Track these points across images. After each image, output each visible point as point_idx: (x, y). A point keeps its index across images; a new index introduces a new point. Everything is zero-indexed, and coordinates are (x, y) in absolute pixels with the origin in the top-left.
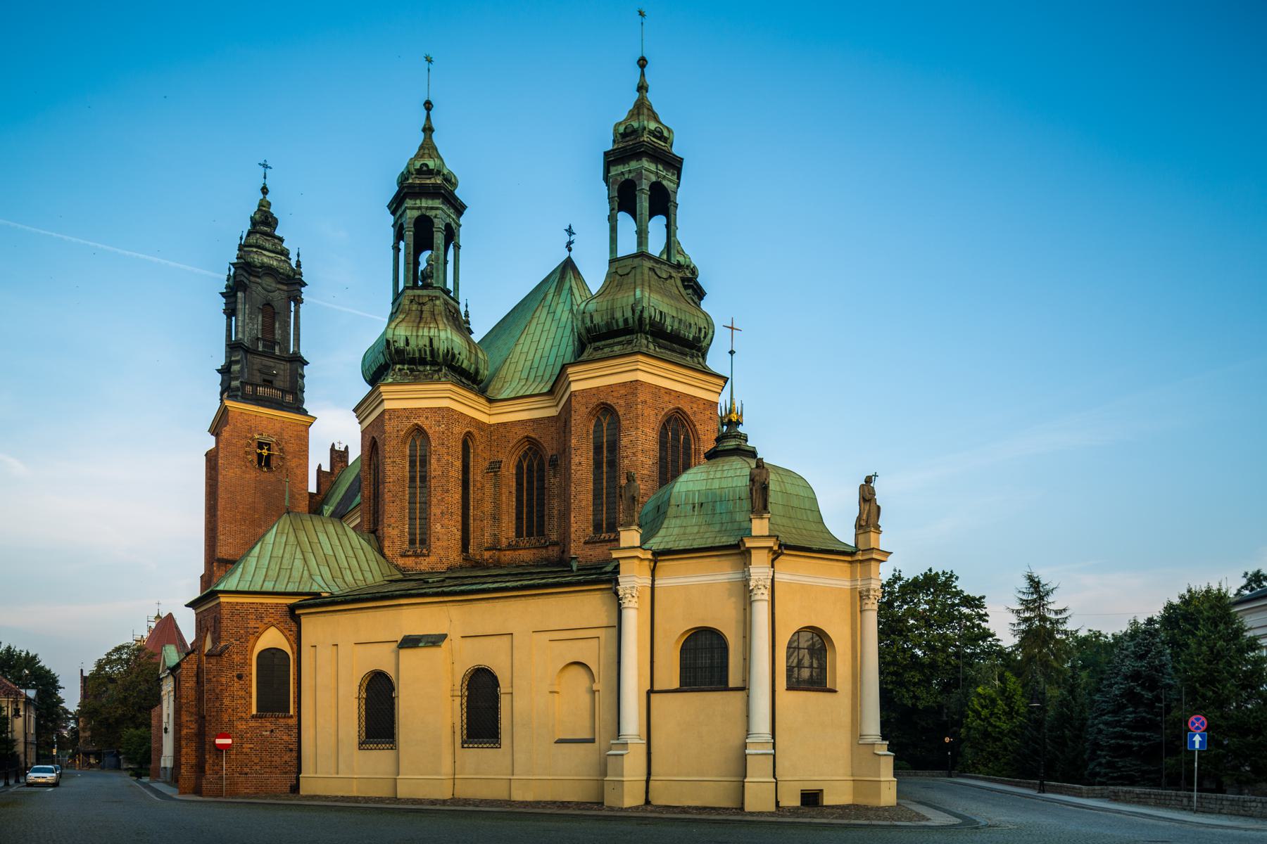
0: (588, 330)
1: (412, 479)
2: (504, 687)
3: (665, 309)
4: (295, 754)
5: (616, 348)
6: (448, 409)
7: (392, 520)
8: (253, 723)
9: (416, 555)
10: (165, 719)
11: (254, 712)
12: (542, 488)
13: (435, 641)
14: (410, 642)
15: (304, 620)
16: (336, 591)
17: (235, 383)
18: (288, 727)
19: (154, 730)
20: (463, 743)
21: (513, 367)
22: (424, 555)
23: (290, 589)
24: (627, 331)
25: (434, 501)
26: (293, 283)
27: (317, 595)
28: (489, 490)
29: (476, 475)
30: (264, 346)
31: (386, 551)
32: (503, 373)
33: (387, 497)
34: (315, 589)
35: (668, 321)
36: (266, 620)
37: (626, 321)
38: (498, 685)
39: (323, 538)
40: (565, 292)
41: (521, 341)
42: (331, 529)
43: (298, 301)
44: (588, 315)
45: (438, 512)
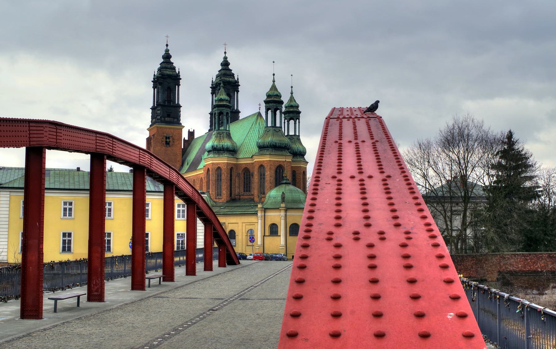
3: (277, 142)
17: (159, 117)
24: (267, 147)
26: (175, 79)
29: (233, 177)
43: (179, 85)
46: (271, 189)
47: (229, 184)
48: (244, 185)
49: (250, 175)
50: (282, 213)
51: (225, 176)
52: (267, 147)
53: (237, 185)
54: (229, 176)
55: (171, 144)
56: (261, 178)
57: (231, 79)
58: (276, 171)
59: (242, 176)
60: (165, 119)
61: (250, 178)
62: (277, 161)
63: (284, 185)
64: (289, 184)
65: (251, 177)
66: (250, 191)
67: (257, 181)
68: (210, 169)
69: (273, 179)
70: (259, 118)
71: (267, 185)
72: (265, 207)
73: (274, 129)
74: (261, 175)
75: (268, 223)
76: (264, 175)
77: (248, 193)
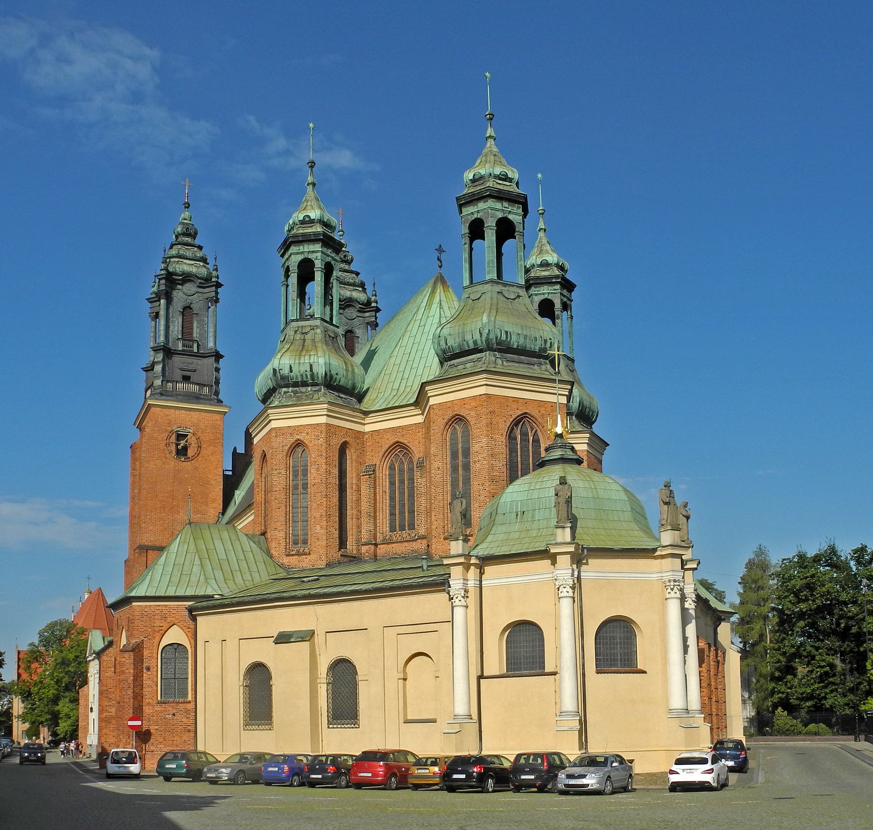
0: (444, 352)
1: (296, 487)
3: (510, 330)
4: (192, 734)
5: (468, 365)
6: (328, 425)
7: (279, 524)
8: (158, 708)
9: (298, 554)
10: (91, 700)
11: (159, 699)
12: (412, 489)
13: (308, 636)
14: (283, 638)
15: (199, 619)
16: (226, 592)
18: (187, 711)
19: (81, 710)
20: (329, 723)
21: (387, 377)
22: (306, 554)
23: (189, 592)
25: (315, 505)
27: (210, 597)
30: (183, 346)
31: (273, 552)
32: (378, 384)
33: (274, 504)
34: (209, 592)
35: (514, 338)
36: (169, 620)
37: (475, 342)
38: (356, 673)
39: (218, 544)
41: (395, 354)
42: (225, 535)
47: (335, 500)
48: (392, 507)
49: (411, 470)
50: (564, 569)
51: (319, 472)
52: (476, 350)
53: (365, 506)
54: (336, 471)
55: (190, 453)
56: (455, 469)
59: (383, 474)
62: (516, 400)
64: (579, 462)
66: (412, 527)
68: (268, 456)
69: (501, 465)
70: (440, 288)
74: (454, 456)
76: (467, 453)
77: (405, 534)
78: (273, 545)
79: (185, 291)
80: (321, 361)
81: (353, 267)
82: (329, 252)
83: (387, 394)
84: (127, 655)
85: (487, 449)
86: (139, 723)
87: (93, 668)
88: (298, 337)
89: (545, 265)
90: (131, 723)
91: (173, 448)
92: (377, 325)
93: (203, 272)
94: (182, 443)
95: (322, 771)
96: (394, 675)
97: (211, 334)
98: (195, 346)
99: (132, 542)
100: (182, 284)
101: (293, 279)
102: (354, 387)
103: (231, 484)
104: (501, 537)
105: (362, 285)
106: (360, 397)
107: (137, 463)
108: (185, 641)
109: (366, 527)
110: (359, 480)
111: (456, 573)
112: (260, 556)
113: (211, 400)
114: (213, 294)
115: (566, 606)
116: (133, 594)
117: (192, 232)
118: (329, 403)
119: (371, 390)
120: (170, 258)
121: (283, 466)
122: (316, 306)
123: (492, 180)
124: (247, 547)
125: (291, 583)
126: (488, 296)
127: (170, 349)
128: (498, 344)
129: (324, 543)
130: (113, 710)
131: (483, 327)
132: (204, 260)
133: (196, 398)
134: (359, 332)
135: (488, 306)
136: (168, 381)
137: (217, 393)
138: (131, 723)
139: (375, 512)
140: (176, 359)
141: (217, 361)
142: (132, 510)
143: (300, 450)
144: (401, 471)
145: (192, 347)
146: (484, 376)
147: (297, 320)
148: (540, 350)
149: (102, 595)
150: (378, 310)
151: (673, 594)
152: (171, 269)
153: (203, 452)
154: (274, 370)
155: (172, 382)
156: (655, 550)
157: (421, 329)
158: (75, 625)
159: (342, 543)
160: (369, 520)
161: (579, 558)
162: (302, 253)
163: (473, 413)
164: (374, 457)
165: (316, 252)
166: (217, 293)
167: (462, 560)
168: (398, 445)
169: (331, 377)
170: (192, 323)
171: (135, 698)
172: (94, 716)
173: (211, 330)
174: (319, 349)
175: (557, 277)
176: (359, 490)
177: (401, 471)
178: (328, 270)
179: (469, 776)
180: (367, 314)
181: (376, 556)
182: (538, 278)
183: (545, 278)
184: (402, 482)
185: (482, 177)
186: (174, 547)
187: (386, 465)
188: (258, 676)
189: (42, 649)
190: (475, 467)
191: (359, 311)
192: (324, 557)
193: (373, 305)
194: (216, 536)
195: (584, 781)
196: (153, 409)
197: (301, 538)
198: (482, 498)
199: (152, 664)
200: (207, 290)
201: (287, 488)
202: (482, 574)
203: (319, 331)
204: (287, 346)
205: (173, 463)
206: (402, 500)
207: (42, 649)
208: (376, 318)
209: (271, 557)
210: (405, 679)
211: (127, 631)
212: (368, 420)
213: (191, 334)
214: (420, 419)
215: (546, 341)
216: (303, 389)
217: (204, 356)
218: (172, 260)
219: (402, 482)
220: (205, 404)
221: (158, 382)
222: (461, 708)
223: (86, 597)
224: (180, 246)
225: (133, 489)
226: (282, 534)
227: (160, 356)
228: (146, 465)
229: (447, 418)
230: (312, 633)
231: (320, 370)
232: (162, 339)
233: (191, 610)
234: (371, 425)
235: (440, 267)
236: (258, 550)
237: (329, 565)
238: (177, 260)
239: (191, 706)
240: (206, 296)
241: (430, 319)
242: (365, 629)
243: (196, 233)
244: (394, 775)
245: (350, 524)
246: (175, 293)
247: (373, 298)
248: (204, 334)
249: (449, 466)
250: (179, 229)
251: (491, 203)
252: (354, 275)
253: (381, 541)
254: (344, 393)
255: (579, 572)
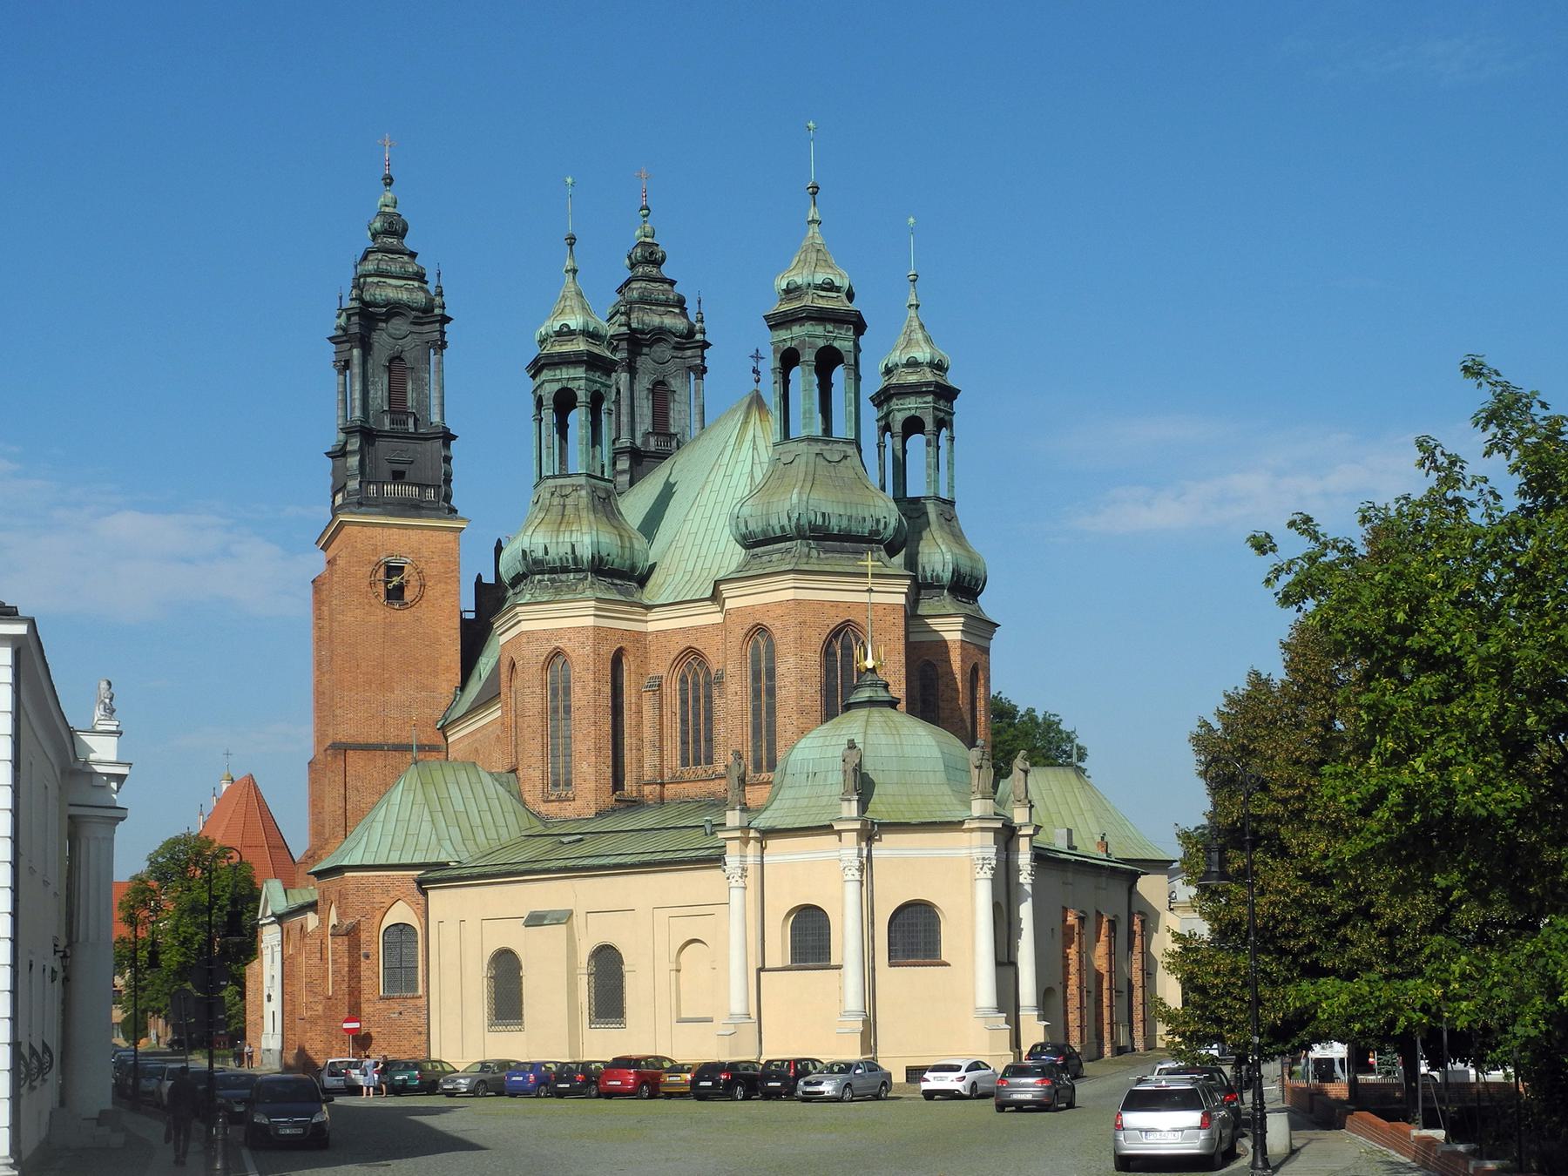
0: (744, 537)
1: (555, 710)
2: (626, 968)
5: (775, 557)
6: (596, 628)
7: (533, 760)
8: (381, 1005)
9: (560, 800)
13: (563, 918)
14: (535, 920)
15: (430, 893)
16: (465, 857)
18: (417, 1008)
21: (678, 552)
25: (580, 736)
28: (649, 713)
30: (392, 422)
31: (526, 796)
32: (667, 561)
33: (527, 733)
34: (443, 858)
35: (834, 522)
37: (782, 528)
39: (454, 790)
40: (747, 444)
41: (691, 517)
42: (463, 776)
44: (742, 520)
45: (584, 748)
46: (803, 732)
47: (607, 728)
48: (685, 733)
50: (848, 849)
51: (587, 692)
53: (648, 733)
54: (607, 689)
55: (409, 595)
56: (757, 694)
57: (668, 321)
58: (828, 651)
60: (380, 492)
61: (709, 698)
63: (862, 713)
64: (893, 704)
65: (715, 693)
66: (710, 760)
67: (736, 706)
70: (755, 416)
71: (786, 719)
72: (763, 821)
73: (817, 448)
74: (756, 677)
75: (781, 904)
76: (771, 674)
77: (700, 769)
78: (526, 787)
79: (392, 331)
80: (585, 539)
81: (667, 271)
82: (597, 376)
83: (678, 578)
84: (339, 940)
85: (797, 673)
86: (356, 1025)
87: (270, 937)
88: (556, 501)
89: (913, 364)
90: (346, 1026)
91: (381, 589)
92: (704, 370)
93: (420, 297)
94: (396, 580)
95: (570, 1079)
96: (665, 966)
97: (435, 401)
98: (411, 421)
99: (320, 736)
100: (386, 321)
101: (549, 415)
102: (633, 568)
103: (474, 636)
104: (788, 804)
105: (680, 302)
106: (642, 581)
107: (325, 609)
108: (414, 922)
109: (650, 760)
110: (640, 698)
111: (733, 849)
112: (509, 803)
113: (438, 509)
114: (437, 335)
115: (852, 891)
116: (345, 863)
117: (399, 228)
118: (598, 600)
119: (657, 569)
120: (365, 276)
121: (537, 683)
122: (578, 459)
123: (811, 291)
124: (491, 792)
125: (547, 844)
126: (803, 459)
127: (371, 430)
128: (812, 531)
129: (592, 785)
130: (320, 1008)
131: (792, 509)
132: (420, 277)
133: (413, 508)
134: (675, 384)
135: (801, 476)
136: (370, 483)
137: (448, 498)
138: (346, 1026)
139: (661, 740)
140: (381, 444)
141: (447, 446)
142: (319, 682)
143: (559, 661)
144: (696, 685)
145: (405, 423)
146: (791, 576)
147: (554, 477)
148: (871, 532)
149: (256, 787)
150: (706, 345)
151: (982, 874)
152: (367, 298)
153: (429, 593)
154: (524, 552)
155: (376, 483)
156: (962, 823)
157: (727, 480)
158: (211, 843)
159: (618, 782)
160: (654, 743)
161: (869, 834)
162: (559, 380)
163: (778, 624)
164: (660, 666)
165: (576, 378)
166: (443, 333)
167: (738, 834)
168: (690, 650)
169: (601, 559)
170: (404, 383)
171: (351, 994)
172: (273, 1008)
173: (435, 394)
174: (585, 522)
175: (928, 384)
176: (639, 712)
177: (696, 685)
178: (596, 401)
179: (716, 1083)
180: (689, 353)
181: (662, 799)
182: (901, 386)
183: (911, 386)
184: (697, 700)
185: (798, 288)
186: (396, 795)
187: (677, 676)
188: (506, 968)
189: (154, 884)
190: (781, 694)
191: (675, 348)
192: (592, 804)
193: (699, 337)
194: (450, 778)
195: (821, 1088)
196: (347, 529)
197: (562, 778)
198: (789, 734)
199: (372, 951)
200: (427, 328)
201: (543, 712)
202: (763, 849)
203: (583, 493)
204: (541, 515)
205: (381, 612)
206: (697, 724)
207: (154, 884)
208: (703, 359)
209: (524, 804)
210: (678, 971)
211: (338, 908)
212: (651, 616)
213: (405, 401)
214: (718, 618)
215: (878, 521)
216: (563, 577)
217: (425, 438)
218: (369, 280)
219: (697, 700)
220: (428, 517)
221: (354, 484)
222: (737, 1007)
223: (225, 787)
224: (379, 256)
225: (318, 649)
226: (538, 773)
227: (354, 444)
228: (340, 617)
229: (747, 627)
230: (571, 913)
231: (585, 552)
232: (358, 413)
233: (420, 883)
234: (656, 623)
235: (758, 381)
236: (507, 795)
237: (600, 814)
238: (376, 280)
239: (423, 1002)
240: (426, 337)
241: (739, 466)
242: (630, 909)
243: (405, 230)
244: (645, 1083)
245: (629, 757)
246: (375, 336)
247: (698, 325)
248: (424, 404)
249: (750, 690)
250: (377, 225)
251: (808, 328)
252: (666, 286)
253: (657, 792)
254: (620, 578)
255: (869, 851)
